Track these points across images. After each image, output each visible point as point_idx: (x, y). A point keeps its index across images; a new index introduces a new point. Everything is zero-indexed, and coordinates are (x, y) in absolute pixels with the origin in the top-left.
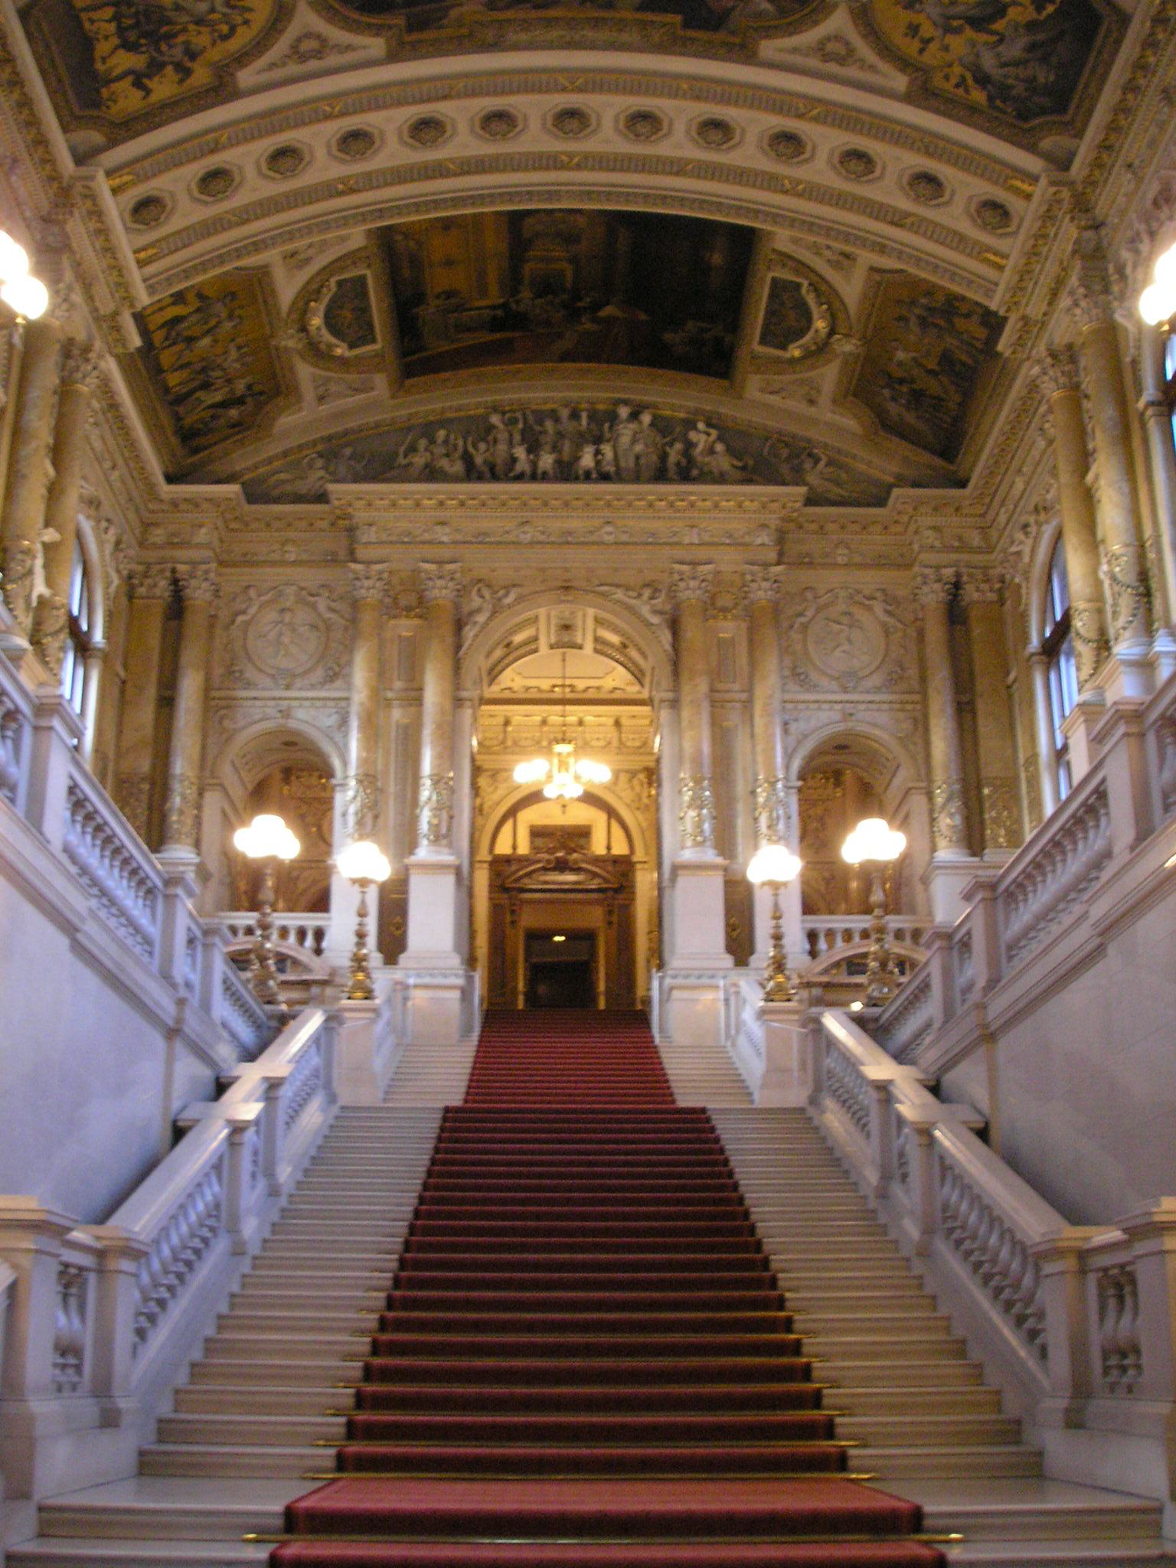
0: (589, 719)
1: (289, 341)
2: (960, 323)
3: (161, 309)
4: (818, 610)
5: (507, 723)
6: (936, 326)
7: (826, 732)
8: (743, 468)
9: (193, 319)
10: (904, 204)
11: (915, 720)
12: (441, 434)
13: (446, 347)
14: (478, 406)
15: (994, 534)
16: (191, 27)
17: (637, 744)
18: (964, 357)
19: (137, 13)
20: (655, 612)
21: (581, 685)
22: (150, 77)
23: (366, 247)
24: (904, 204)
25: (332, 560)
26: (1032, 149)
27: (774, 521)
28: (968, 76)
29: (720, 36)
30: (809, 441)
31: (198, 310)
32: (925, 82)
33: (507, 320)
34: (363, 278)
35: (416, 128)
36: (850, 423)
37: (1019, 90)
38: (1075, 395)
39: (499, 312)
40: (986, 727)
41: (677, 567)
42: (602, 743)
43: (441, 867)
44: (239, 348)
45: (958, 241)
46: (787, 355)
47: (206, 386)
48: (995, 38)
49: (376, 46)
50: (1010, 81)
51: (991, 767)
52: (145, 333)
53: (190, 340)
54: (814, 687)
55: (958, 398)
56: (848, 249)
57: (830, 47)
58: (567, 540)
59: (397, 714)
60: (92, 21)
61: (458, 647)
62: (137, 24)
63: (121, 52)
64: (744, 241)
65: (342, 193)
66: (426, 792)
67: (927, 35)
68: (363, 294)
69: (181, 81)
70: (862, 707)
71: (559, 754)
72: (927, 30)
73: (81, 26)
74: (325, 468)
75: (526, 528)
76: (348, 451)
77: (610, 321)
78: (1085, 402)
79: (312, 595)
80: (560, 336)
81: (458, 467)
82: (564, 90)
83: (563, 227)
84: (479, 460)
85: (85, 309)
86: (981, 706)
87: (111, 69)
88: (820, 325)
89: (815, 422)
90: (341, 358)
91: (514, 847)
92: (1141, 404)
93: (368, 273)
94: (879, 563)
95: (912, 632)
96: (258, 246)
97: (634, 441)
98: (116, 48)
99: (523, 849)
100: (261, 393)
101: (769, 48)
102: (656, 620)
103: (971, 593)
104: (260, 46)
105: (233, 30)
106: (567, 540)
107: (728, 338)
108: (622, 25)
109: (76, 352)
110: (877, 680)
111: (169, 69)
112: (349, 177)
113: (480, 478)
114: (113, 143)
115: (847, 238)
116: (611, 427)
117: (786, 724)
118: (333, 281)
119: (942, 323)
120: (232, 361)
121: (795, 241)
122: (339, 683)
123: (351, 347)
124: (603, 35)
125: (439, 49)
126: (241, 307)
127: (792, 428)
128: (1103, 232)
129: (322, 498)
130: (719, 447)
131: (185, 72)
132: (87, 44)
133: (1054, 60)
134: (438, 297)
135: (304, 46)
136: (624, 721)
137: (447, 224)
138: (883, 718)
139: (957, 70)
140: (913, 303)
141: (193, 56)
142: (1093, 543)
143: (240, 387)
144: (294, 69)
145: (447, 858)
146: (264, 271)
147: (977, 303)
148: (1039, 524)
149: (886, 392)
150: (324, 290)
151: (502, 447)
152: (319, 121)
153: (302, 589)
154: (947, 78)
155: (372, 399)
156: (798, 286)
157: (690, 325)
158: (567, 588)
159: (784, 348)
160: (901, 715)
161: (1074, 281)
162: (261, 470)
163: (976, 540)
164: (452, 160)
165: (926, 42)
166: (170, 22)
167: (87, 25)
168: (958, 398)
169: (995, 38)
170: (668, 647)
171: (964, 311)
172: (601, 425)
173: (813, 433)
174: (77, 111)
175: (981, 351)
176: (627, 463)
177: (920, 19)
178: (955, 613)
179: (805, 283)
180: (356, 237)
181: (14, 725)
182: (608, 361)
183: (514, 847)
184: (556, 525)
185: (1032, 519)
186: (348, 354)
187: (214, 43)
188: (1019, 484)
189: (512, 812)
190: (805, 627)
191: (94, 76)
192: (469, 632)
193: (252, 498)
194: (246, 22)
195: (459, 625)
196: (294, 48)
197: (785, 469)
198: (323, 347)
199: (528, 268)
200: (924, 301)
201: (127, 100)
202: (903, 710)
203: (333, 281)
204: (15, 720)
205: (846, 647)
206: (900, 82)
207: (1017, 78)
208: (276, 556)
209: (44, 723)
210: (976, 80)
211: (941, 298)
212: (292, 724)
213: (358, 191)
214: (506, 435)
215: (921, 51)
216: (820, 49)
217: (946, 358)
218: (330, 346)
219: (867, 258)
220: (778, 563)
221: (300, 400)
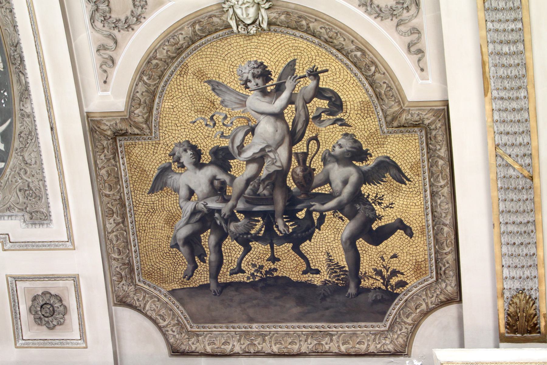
16: (300, 147)
60: (240, 270)
63: (305, 247)
69: (401, 178)
73: (239, 285)
87: (333, 267)
98: (296, 249)
104: (364, 63)
105: (319, 93)
111: (366, 189)
131: (387, 168)
166: (279, 176)
167: (239, 278)
187: (343, 123)
191: (333, 290)
194: (314, 74)
201: (403, 253)
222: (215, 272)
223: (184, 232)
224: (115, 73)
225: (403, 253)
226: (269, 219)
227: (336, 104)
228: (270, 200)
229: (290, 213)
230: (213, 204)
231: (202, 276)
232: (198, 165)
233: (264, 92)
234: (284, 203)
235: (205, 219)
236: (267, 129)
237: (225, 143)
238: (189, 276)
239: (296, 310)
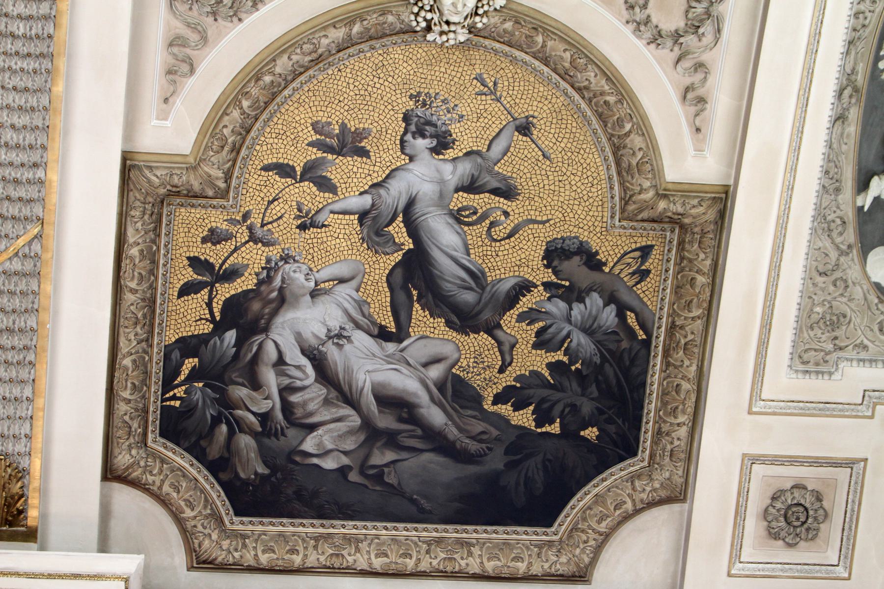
28: (246, 283)
37: (258, 402)
48: (390, 324)
50: (270, 379)
133: (381, 457)
165: (312, 173)
169: (390, 324)
177: (385, 153)
207: (285, 391)
210: (231, 304)
215: (284, 170)
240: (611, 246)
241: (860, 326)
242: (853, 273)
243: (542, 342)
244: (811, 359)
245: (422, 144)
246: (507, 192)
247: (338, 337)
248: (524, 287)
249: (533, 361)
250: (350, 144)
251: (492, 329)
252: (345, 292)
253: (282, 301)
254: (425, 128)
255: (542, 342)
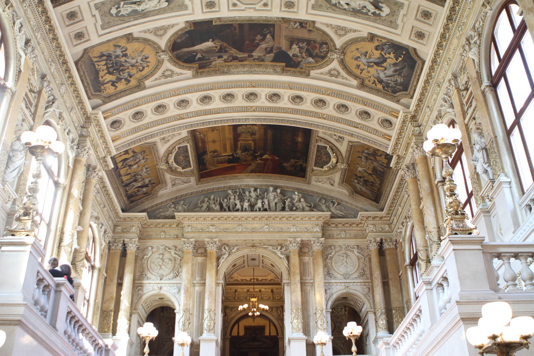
0: (263, 290)
1: (163, 166)
2: (378, 158)
3: (121, 156)
4: (336, 252)
5: (236, 291)
6: (371, 159)
7: (339, 293)
8: (310, 207)
9: (132, 159)
10: (358, 121)
11: (369, 288)
12: (212, 197)
13: (214, 168)
14: (224, 187)
15: (393, 226)
16: (130, 67)
17: (279, 298)
18: (380, 169)
19: (113, 63)
20: (282, 254)
21: (260, 278)
22: (117, 83)
23: (187, 137)
24: (358, 121)
25: (177, 237)
26: (398, 102)
27: (321, 223)
28: (376, 80)
29: (298, 69)
30: (332, 197)
31: (133, 156)
32: (363, 82)
33: (233, 159)
34: (187, 146)
35: (203, 100)
36: (345, 191)
37: (392, 84)
38: (416, 179)
39: (231, 157)
40: (393, 290)
41: (289, 239)
42: (267, 298)
43: (210, 340)
44: (146, 169)
45: (376, 132)
46: (324, 170)
47: (136, 181)
49: (189, 73)
50: (389, 82)
51: (395, 304)
52: (115, 163)
53: (130, 166)
54: (335, 278)
55: (379, 182)
56: (341, 135)
57: (332, 72)
58: (253, 231)
59: (197, 288)
60: (98, 65)
61: (218, 266)
62: (113, 67)
63: (108, 75)
64: (307, 133)
65: (179, 119)
66: (206, 315)
67: (362, 68)
68: (187, 151)
69: (127, 84)
70: (351, 284)
71: (252, 302)
72: (362, 67)
74: (175, 208)
75: (240, 227)
76: (182, 202)
77: (266, 160)
78: (418, 182)
79: (169, 249)
80: (250, 165)
81: (218, 207)
82: (249, 87)
83: (250, 129)
84: (224, 205)
85: (95, 156)
86: (391, 283)
88: (334, 160)
89: (333, 191)
90: (180, 172)
91: (238, 333)
92: (436, 182)
93: (188, 145)
94: (356, 237)
95: (367, 259)
96: (152, 136)
97: (275, 198)
99: (242, 333)
100: (154, 183)
101: (313, 73)
102: (282, 256)
103: (386, 246)
104: (152, 74)
105: (144, 68)
106: (253, 231)
107: (304, 165)
108: (266, 67)
109: (91, 169)
110: (356, 275)
111: (123, 80)
112: (181, 114)
113: (225, 211)
114: (105, 103)
115: (341, 132)
116: (267, 194)
117: (326, 290)
118: (176, 147)
119: (372, 158)
120: (144, 173)
121: (325, 133)
122: (178, 278)
123: (183, 168)
124: (261, 69)
125: (209, 74)
126: (147, 155)
127: (326, 193)
128: (421, 128)
129: (173, 217)
130: (302, 200)
132: (97, 72)
134: (211, 152)
135: (167, 73)
136: (274, 290)
137: (213, 129)
138: (359, 288)
139: (372, 78)
140: (363, 152)
141: (131, 76)
142: (424, 228)
143: (147, 181)
144: (163, 80)
145: (213, 337)
146: (154, 144)
147: (383, 152)
148: (407, 222)
149: (356, 181)
150: (174, 150)
151: (231, 200)
152: (171, 97)
153: (166, 247)
154: (369, 81)
155: (190, 184)
156: (326, 147)
157: (292, 161)
158: (253, 246)
159: (322, 167)
160: (364, 287)
161: (412, 144)
162: (153, 208)
163: (387, 228)
164: (214, 109)
165: (362, 70)
167: (97, 66)
168: (379, 182)
170: (286, 265)
171: (379, 154)
172: (263, 193)
173: (333, 194)
174: (94, 93)
175: (385, 167)
176: (273, 204)
178: (381, 252)
179: (328, 147)
180: (184, 133)
181: (48, 290)
182: (266, 173)
183: (238, 333)
184: (249, 226)
185: (404, 221)
186: (182, 171)
187: (137, 72)
188: (400, 210)
189: (238, 322)
190: (331, 258)
191: (99, 82)
192: (222, 261)
193: (150, 218)
194: (148, 66)
195: (218, 259)
196: (163, 74)
197: (324, 207)
198: (173, 168)
199: (239, 143)
200: (366, 151)
201: (110, 90)
202: (365, 285)
203: (176, 147)
204: (49, 288)
205: (345, 264)
206: (355, 82)
207: (391, 81)
208: (158, 236)
209: (58, 289)
210: (379, 82)
211: (372, 150)
212: (162, 292)
213: (184, 119)
214: (233, 197)
215: (361, 73)
216: (329, 73)
217: (375, 170)
218: (176, 168)
219: (347, 138)
220: (322, 237)
221: (166, 185)
222: (96, 62)
223: (105, 53)
224: (143, 33)
225: (110, 90)
226: (113, 67)
227: (141, 71)
228: (116, 65)
229: (115, 70)
230: (113, 57)
231: (95, 60)
232: (122, 52)
233: (142, 59)
234: (116, 66)
235: (109, 56)
236: (134, 61)
237: (129, 55)
238: (94, 57)
239: (92, 78)
240: (377, 43)
241: (392, 19)
242: (384, 18)
243: (390, 54)
244: (396, 27)
245: (359, 59)
246: (367, 52)
247: (385, 74)
248: (381, 54)
249: (392, 55)
250: (358, 66)
251: (387, 58)
252: (379, 71)
253: (379, 78)
254: (357, 59)
255: (390, 54)
